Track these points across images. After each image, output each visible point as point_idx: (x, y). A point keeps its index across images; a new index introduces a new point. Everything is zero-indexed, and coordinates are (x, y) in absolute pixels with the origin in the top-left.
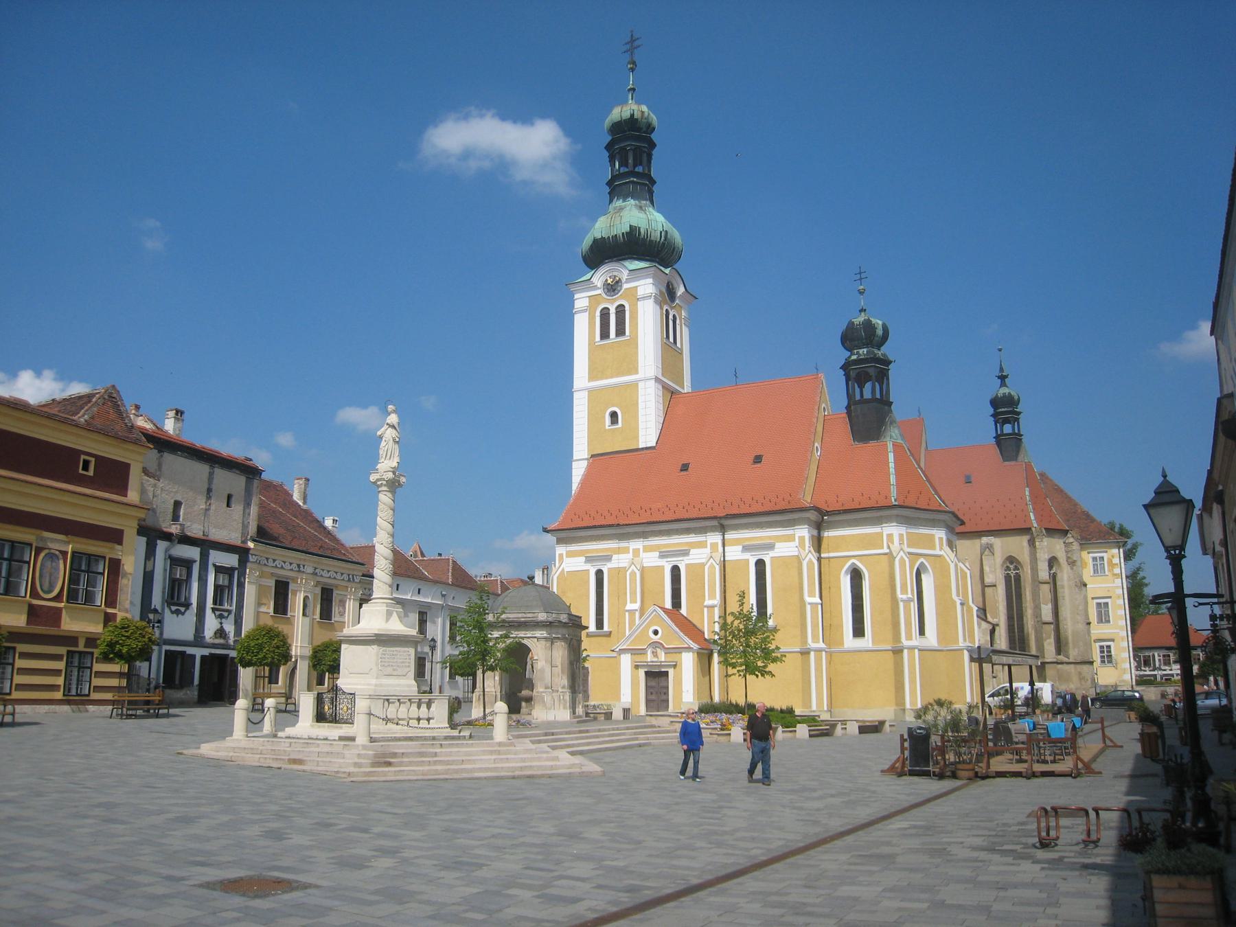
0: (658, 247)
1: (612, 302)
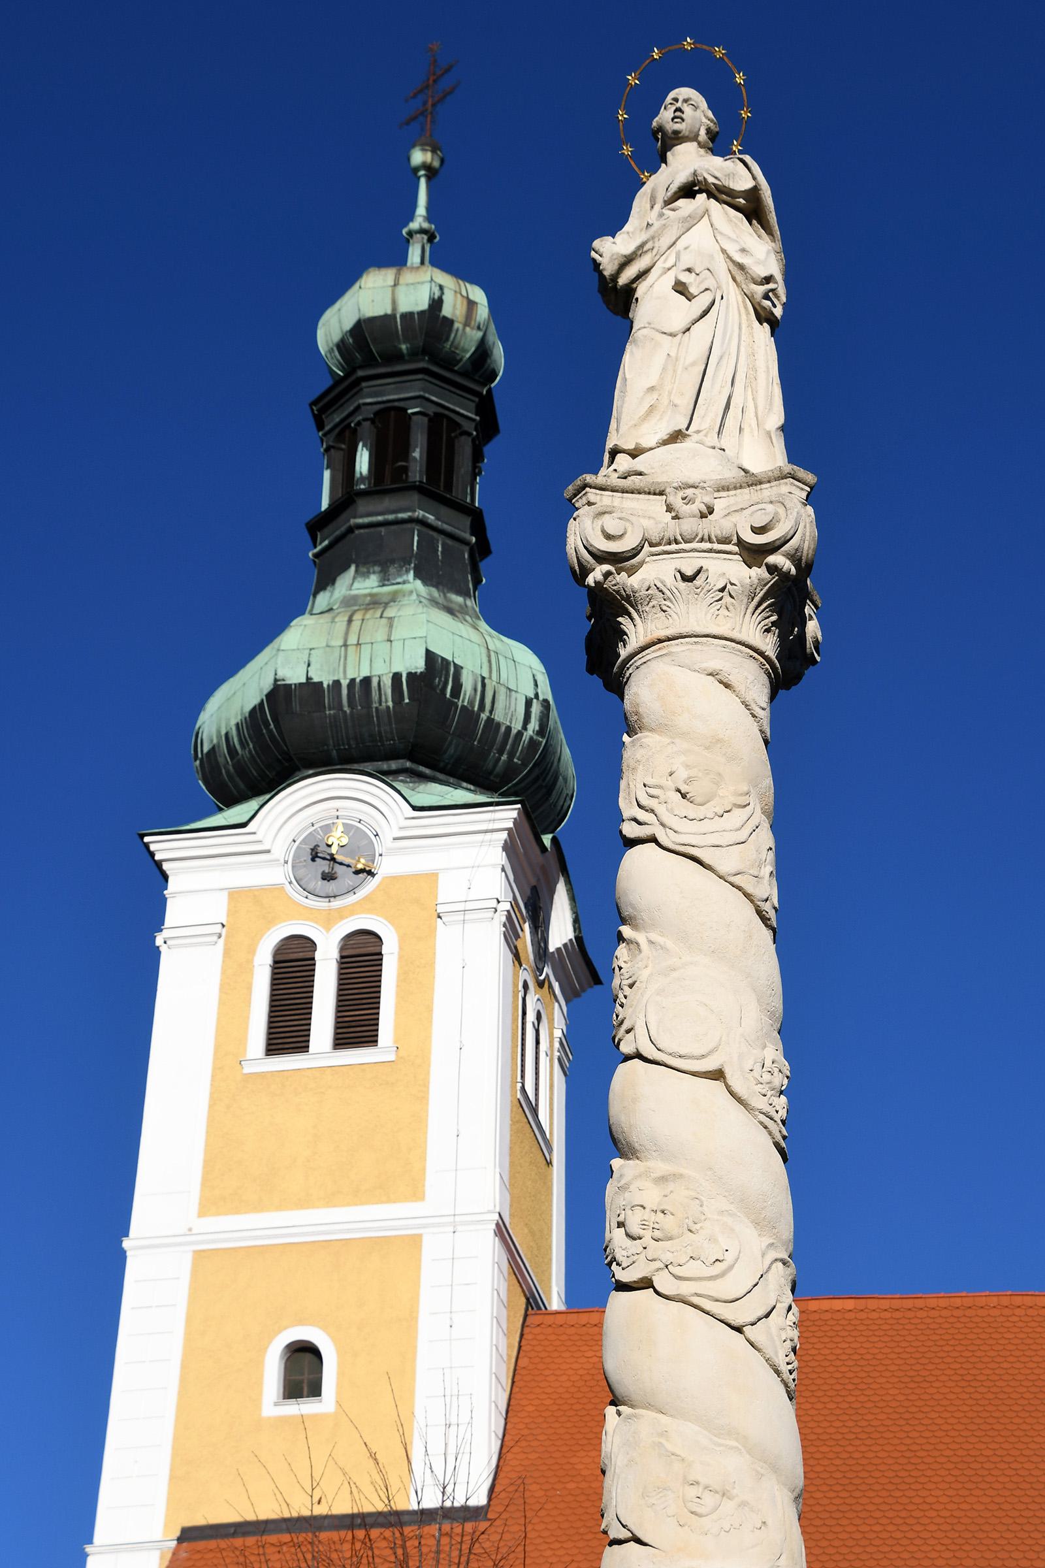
0: (512, 755)
1: (328, 922)
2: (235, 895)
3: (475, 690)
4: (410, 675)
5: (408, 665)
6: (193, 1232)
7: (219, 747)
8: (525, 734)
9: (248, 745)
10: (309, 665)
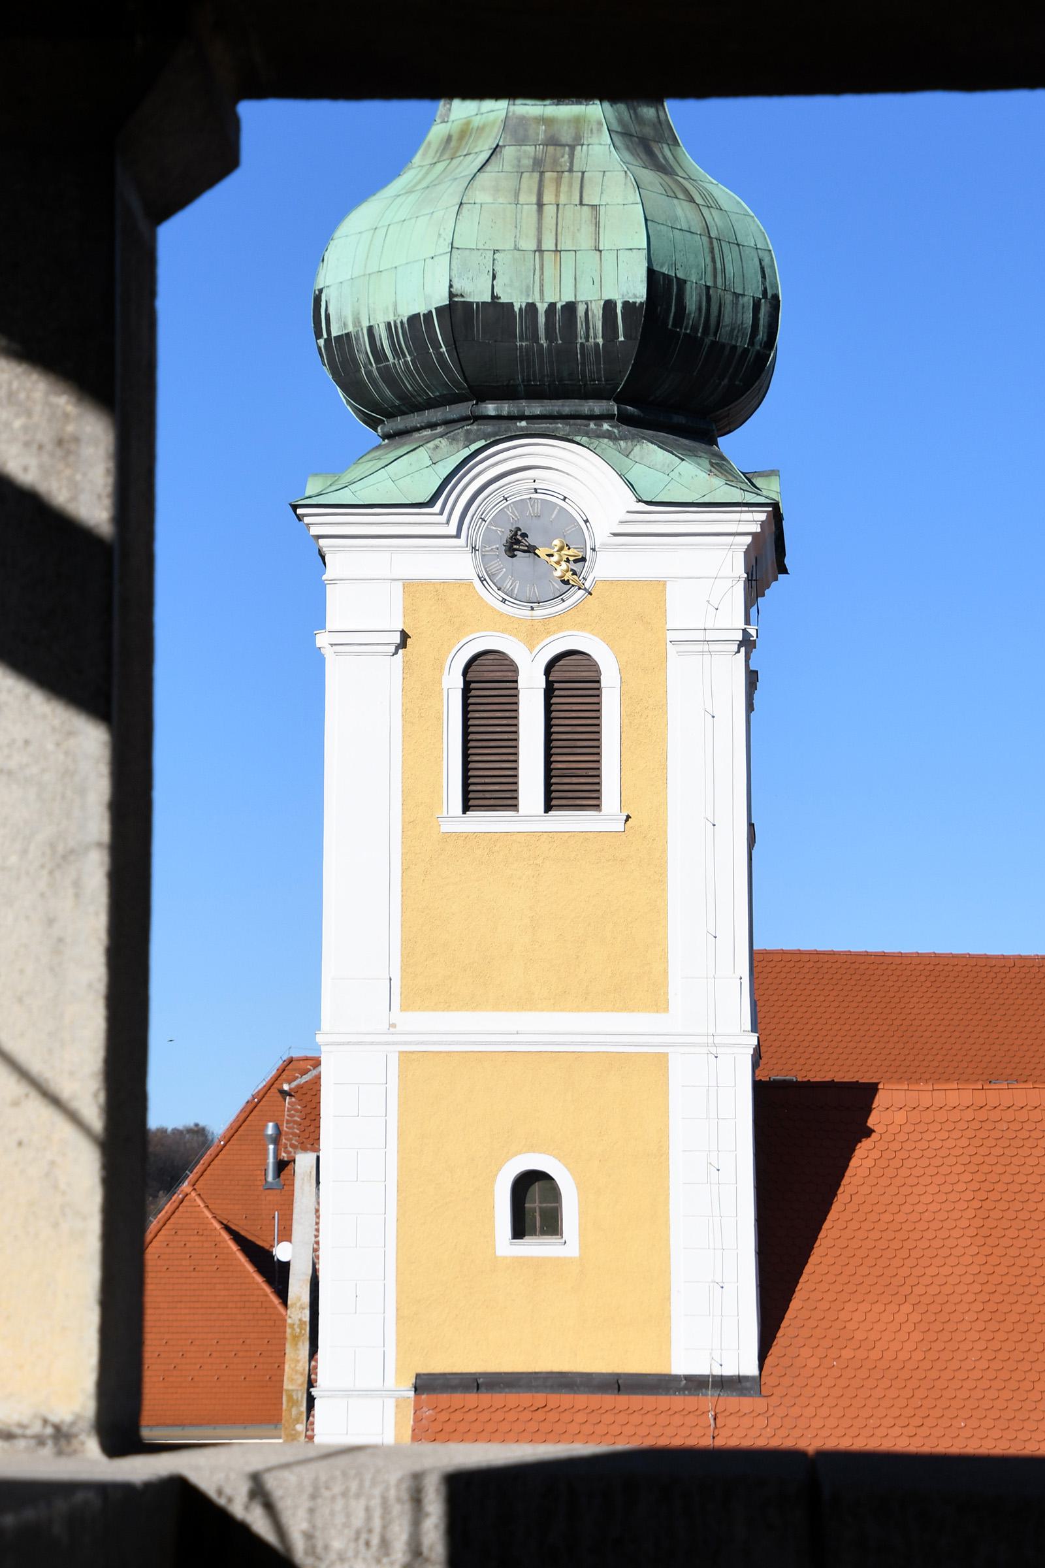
2: (411, 586)
3: (700, 309)
4: (626, 304)
5: (624, 290)
6: (398, 1029)
7: (357, 339)
8: (751, 350)
9: (404, 356)
10: (494, 277)
